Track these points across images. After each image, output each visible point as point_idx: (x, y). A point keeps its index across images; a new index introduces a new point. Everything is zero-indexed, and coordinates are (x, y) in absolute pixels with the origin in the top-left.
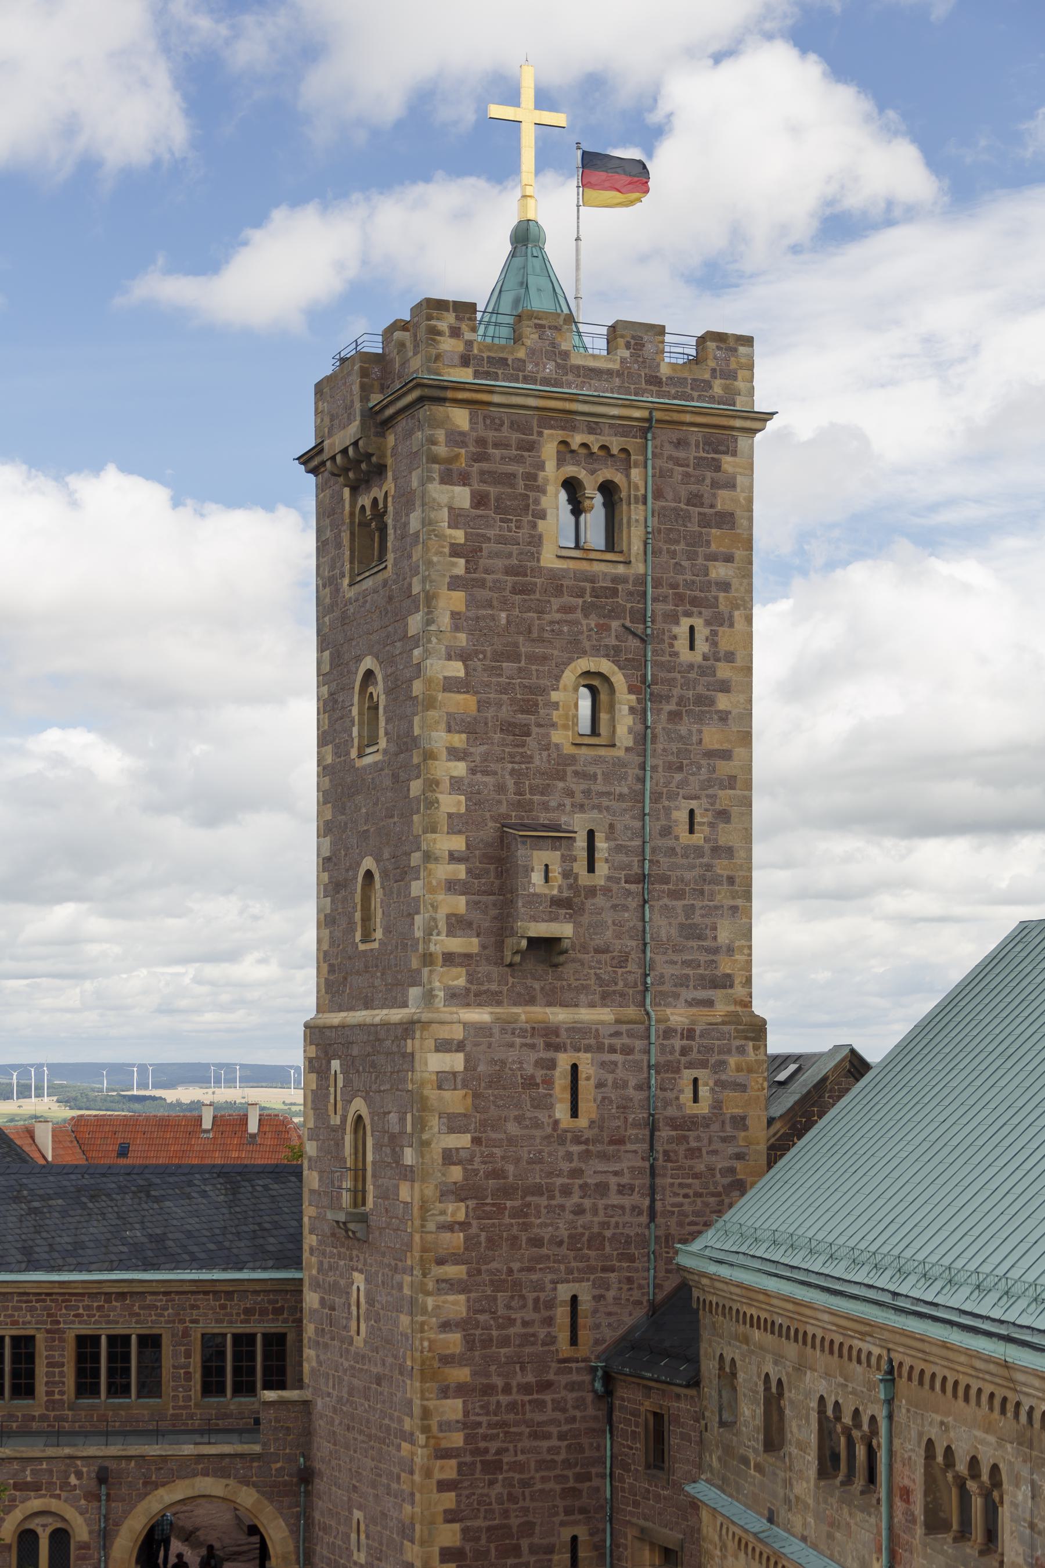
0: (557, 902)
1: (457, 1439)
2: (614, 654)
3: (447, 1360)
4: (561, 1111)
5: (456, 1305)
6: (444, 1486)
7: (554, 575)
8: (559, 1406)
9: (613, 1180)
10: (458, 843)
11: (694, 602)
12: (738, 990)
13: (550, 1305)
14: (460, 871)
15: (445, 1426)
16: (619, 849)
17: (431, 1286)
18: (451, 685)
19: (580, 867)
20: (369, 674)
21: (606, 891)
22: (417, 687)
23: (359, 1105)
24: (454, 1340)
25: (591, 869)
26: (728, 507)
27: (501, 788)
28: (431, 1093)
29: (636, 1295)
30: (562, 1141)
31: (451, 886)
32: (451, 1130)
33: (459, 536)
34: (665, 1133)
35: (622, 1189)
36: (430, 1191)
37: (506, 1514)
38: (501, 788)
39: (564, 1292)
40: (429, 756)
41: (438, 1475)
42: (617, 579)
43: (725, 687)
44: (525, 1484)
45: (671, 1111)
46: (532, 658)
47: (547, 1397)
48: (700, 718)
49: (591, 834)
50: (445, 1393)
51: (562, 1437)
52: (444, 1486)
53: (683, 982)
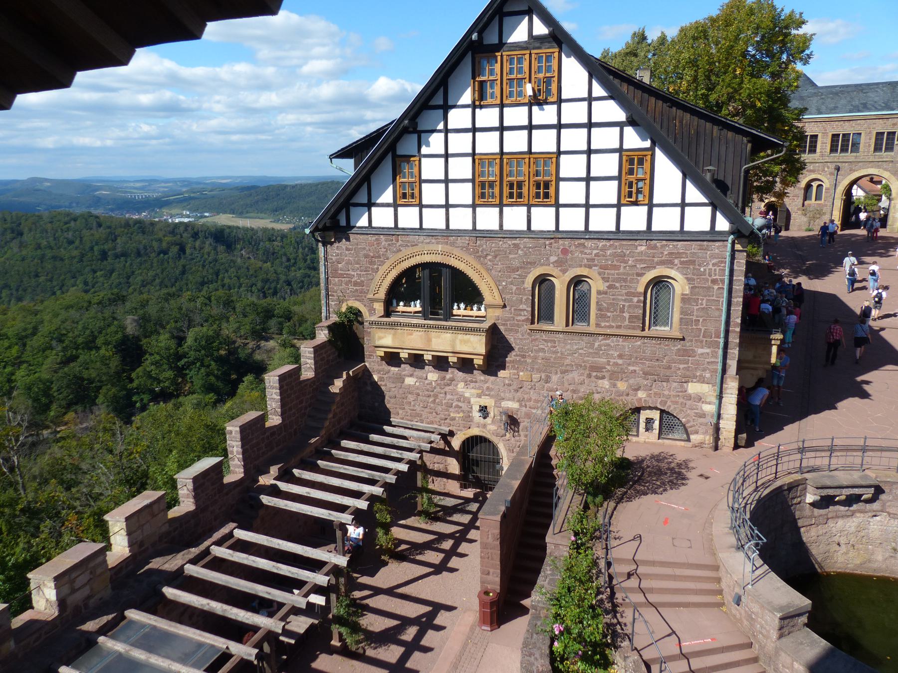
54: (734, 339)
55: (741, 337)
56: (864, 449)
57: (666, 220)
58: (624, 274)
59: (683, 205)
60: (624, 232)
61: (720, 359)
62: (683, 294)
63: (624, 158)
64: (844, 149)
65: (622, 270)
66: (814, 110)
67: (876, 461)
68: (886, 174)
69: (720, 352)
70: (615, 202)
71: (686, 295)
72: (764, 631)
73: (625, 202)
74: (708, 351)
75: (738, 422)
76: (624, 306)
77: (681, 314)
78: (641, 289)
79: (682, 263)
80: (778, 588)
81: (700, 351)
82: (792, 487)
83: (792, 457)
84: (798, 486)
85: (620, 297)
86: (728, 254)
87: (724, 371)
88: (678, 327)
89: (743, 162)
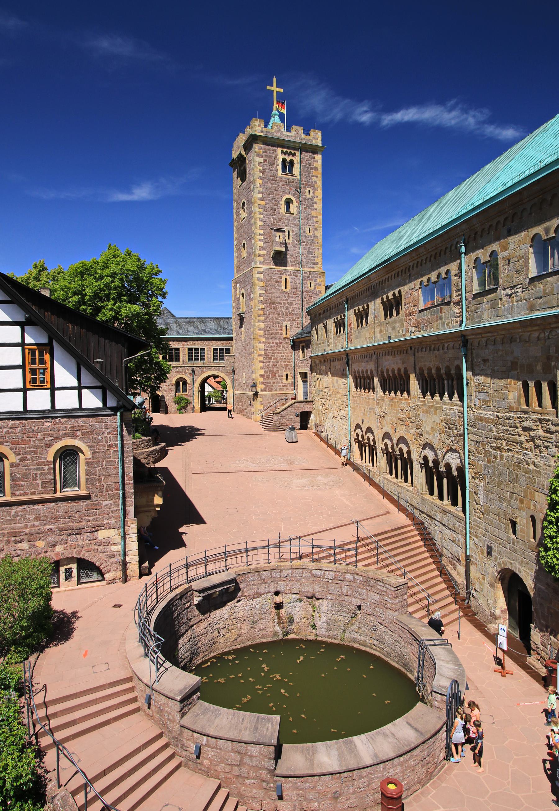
0: (281, 243)
1: (263, 353)
2: (293, 195)
3: (260, 336)
4: (283, 287)
5: (262, 325)
6: (260, 362)
7: (280, 177)
8: (284, 347)
9: (294, 302)
10: (261, 232)
11: (310, 185)
12: (319, 266)
13: (281, 327)
14: (262, 237)
15: (260, 350)
16: (295, 235)
17: (257, 321)
18: (259, 199)
19: (287, 238)
20: (244, 203)
21: (292, 243)
22: (252, 200)
23: (243, 290)
24: (262, 333)
25: (289, 239)
26: (317, 166)
27: (270, 221)
28: (257, 282)
29: (299, 326)
30: (283, 293)
31: (260, 240)
32: (261, 290)
33: (261, 168)
34: (304, 293)
35: (296, 304)
36: (257, 302)
37: (273, 368)
38: (270, 221)
39: (284, 324)
40: (255, 213)
41: (259, 359)
42: (293, 179)
43: (316, 203)
44: (277, 362)
45: (306, 289)
46: (276, 194)
47: (281, 345)
48: (311, 209)
49: (289, 231)
50: (260, 343)
51: (284, 353)
52: (260, 362)
53: (308, 263)
54: (130, 490)
55: (135, 488)
56: (226, 555)
57: (67, 400)
58: (34, 447)
59: (79, 388)
60: (31, 411)
61: (121, 507)
62: (86, 459)
63: (27, 351)
64: (197, 359)
65: (32, 444)
66: (175, 333)
67: (234, 561)
68: (222, 375)
69: (121, 501)
70: (21, 386)
71: (89, 459)
72: (171, 717)
73: (30, 387)
74: (111, 502)
75: (140, 555)
76: (36, 474)
77: (87, 474)
78: (50, 458)
79: (83, 434)
80: (177, 677)
81: (105, 503)
82: (183, 595)
83: (180, 572)
84: (187, 593)
85: (31, 467)
86: (118, 424)
87: (125, 515)
88: (85, 486)
89: (123, 357)
